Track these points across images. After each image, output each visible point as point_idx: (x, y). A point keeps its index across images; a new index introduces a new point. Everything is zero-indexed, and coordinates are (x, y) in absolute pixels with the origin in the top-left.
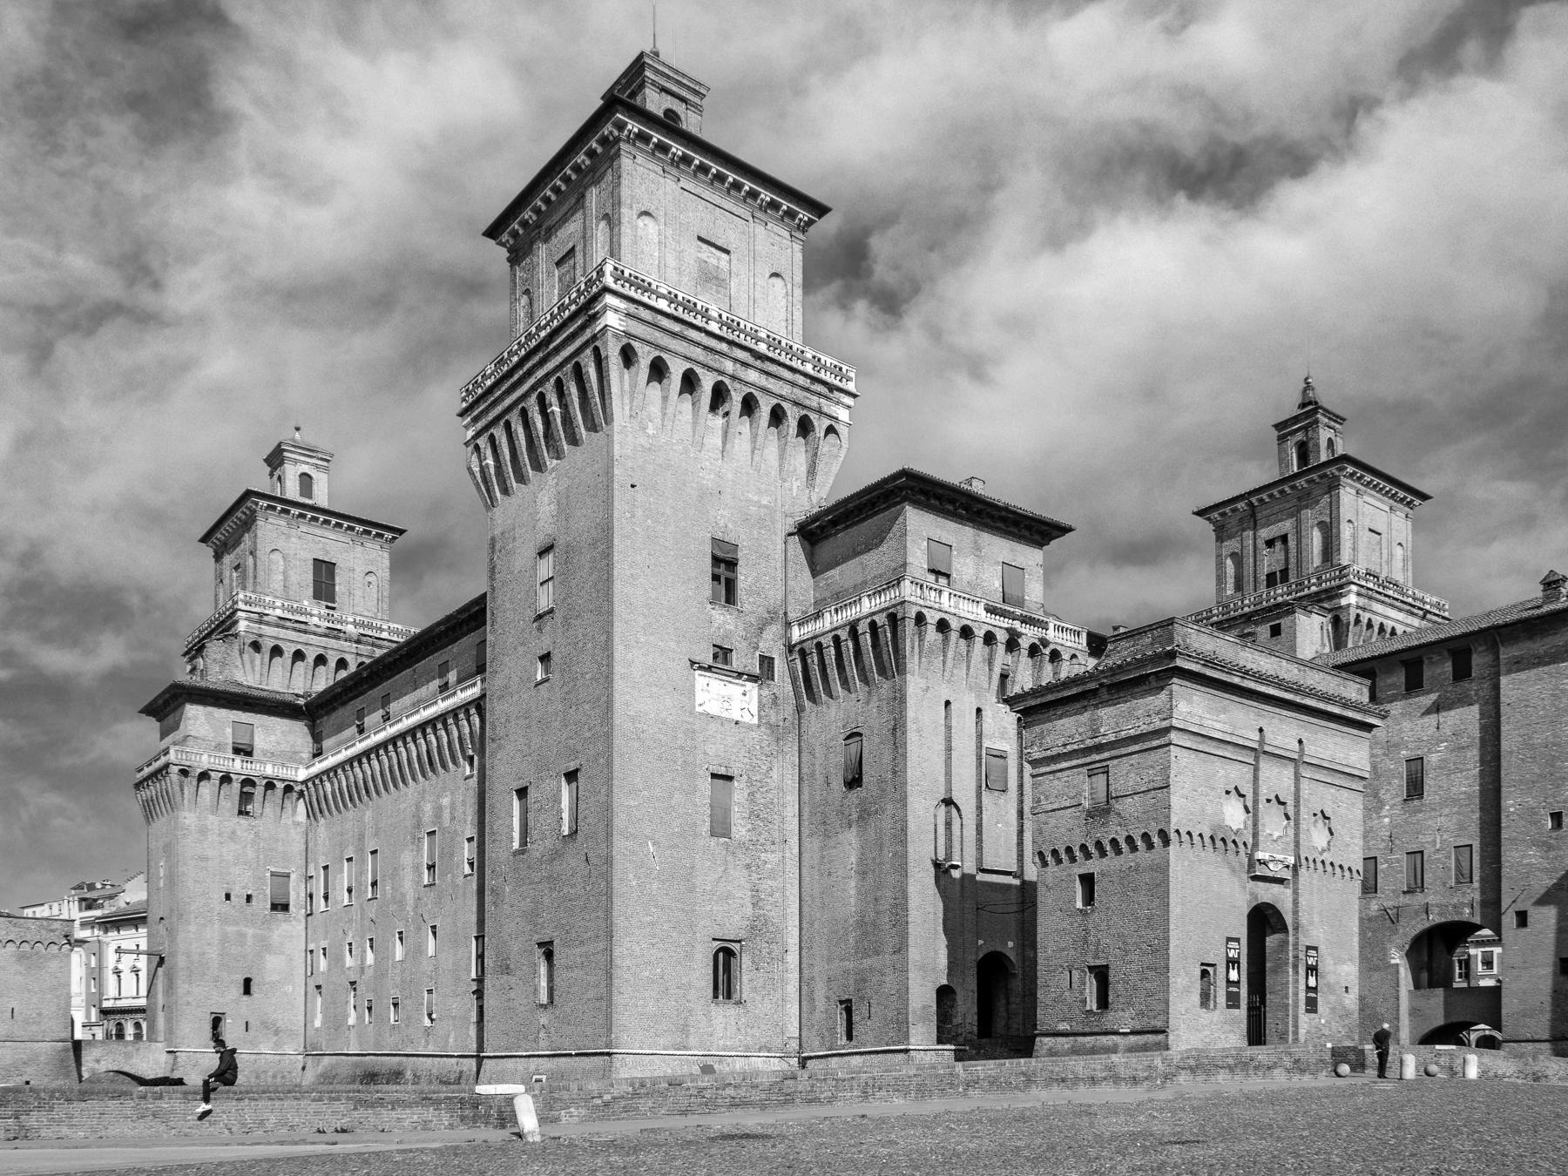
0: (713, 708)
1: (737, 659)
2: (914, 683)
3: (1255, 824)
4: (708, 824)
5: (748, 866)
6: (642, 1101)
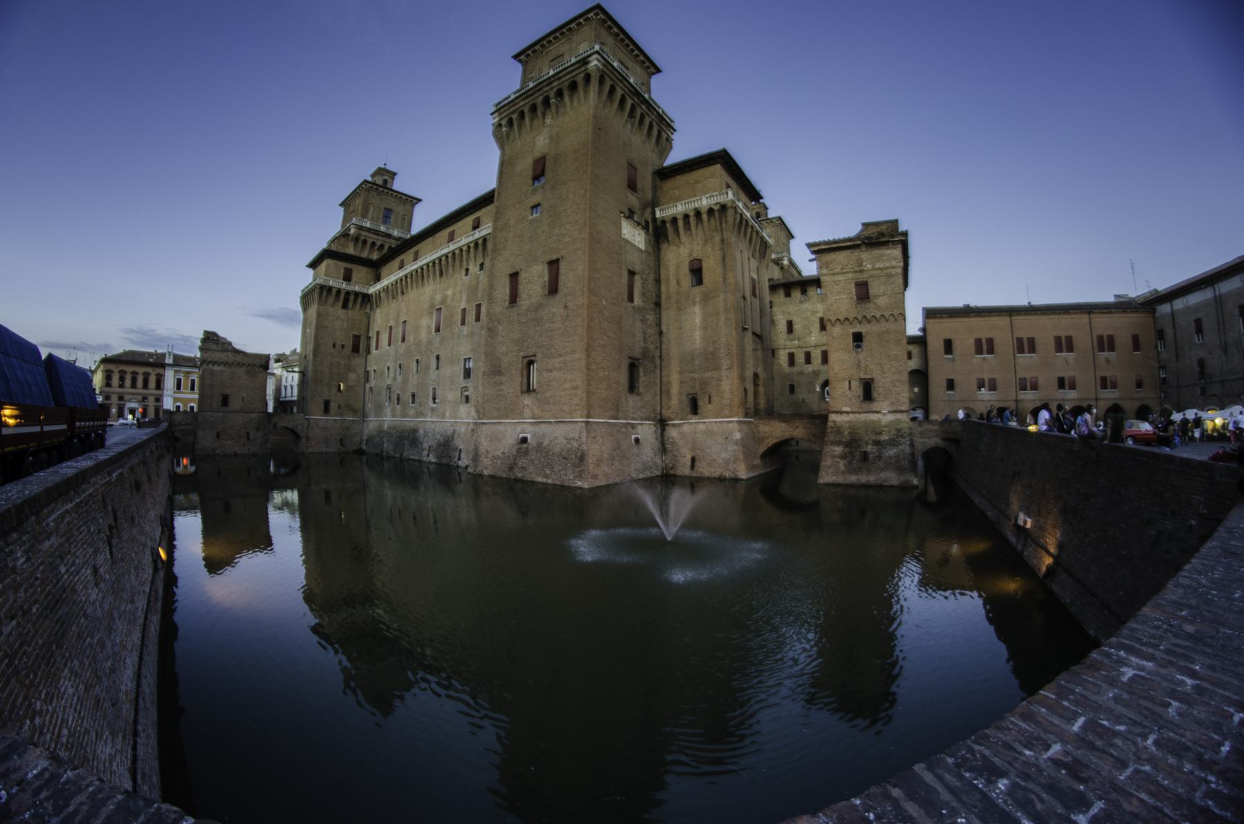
4: (626, 295)
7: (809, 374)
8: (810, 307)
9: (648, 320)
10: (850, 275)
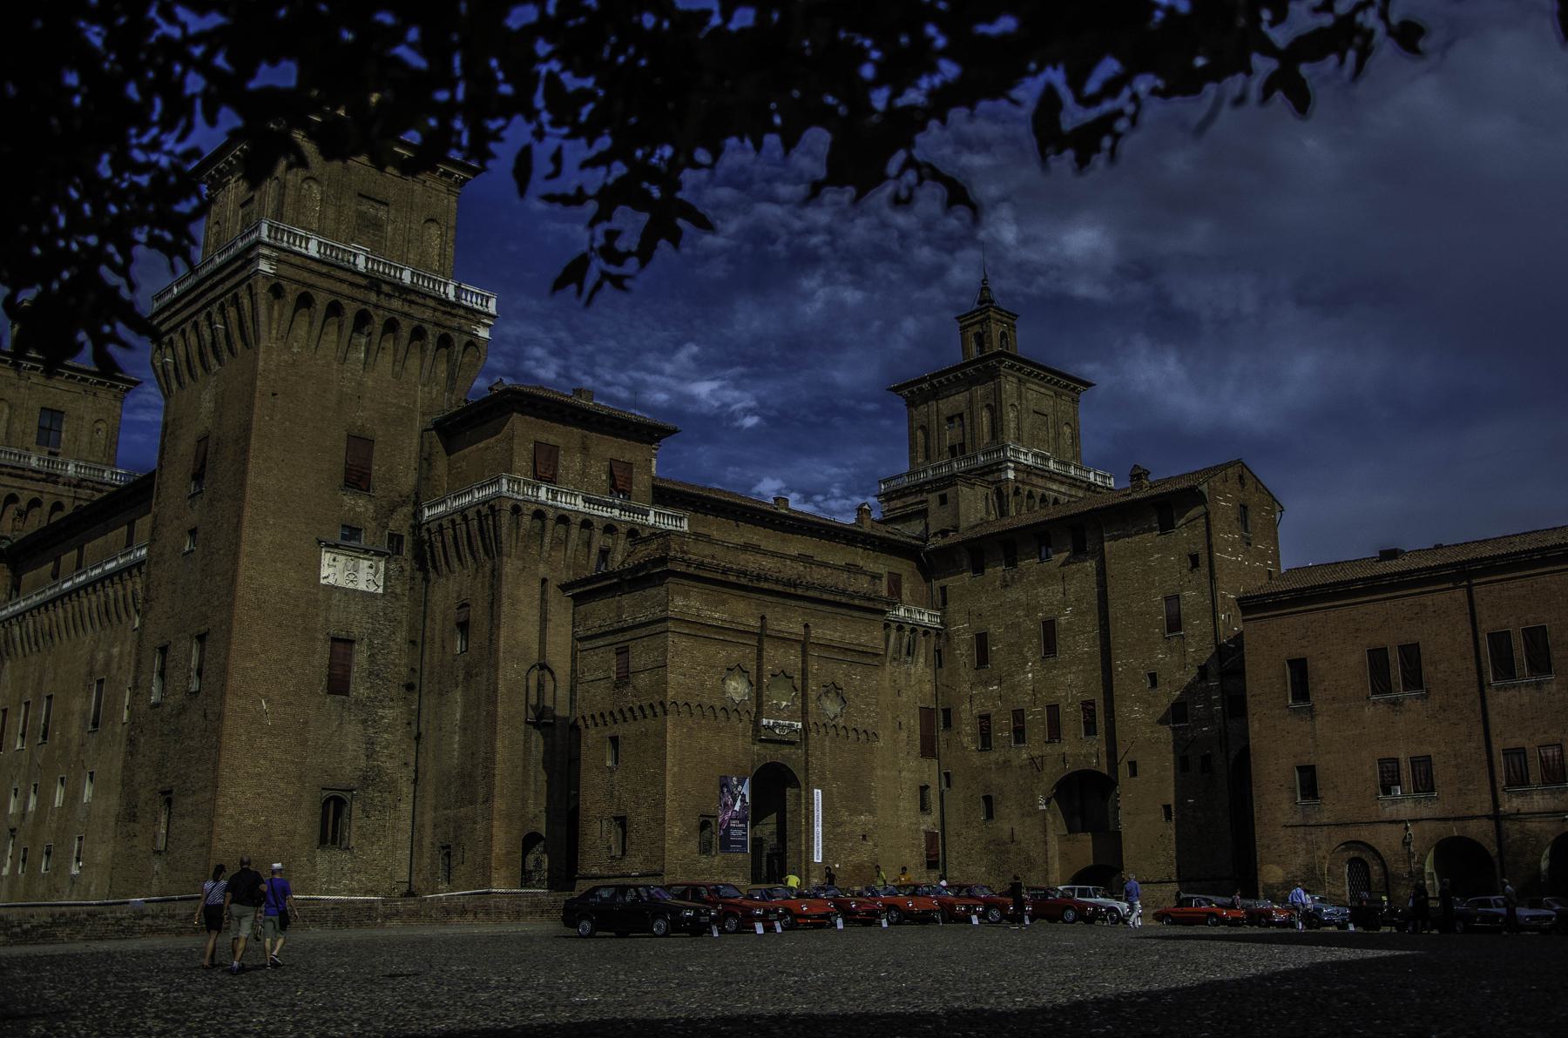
0: (342, 582)
1: (366, 537)
2: (510, 567)
3: (759, 696)
5: (364, 722)
6: (60, 929)
7: (1021, 767)
8: (1023, 598)
9: (383, 718)
10: (611, 639)
